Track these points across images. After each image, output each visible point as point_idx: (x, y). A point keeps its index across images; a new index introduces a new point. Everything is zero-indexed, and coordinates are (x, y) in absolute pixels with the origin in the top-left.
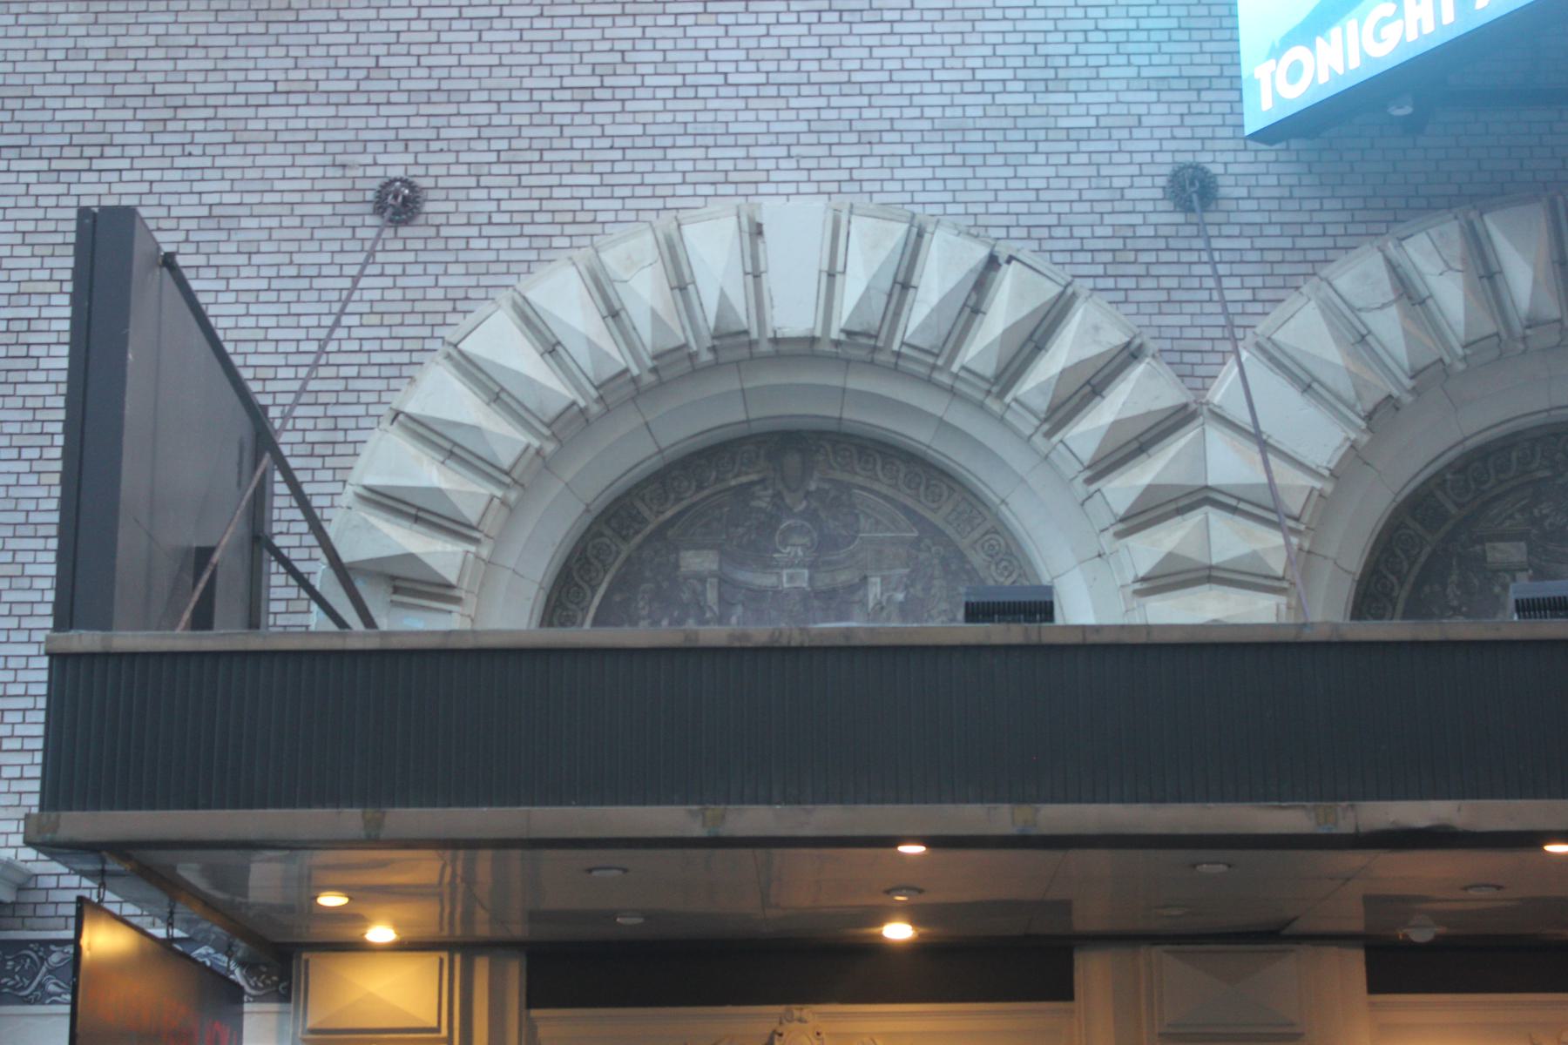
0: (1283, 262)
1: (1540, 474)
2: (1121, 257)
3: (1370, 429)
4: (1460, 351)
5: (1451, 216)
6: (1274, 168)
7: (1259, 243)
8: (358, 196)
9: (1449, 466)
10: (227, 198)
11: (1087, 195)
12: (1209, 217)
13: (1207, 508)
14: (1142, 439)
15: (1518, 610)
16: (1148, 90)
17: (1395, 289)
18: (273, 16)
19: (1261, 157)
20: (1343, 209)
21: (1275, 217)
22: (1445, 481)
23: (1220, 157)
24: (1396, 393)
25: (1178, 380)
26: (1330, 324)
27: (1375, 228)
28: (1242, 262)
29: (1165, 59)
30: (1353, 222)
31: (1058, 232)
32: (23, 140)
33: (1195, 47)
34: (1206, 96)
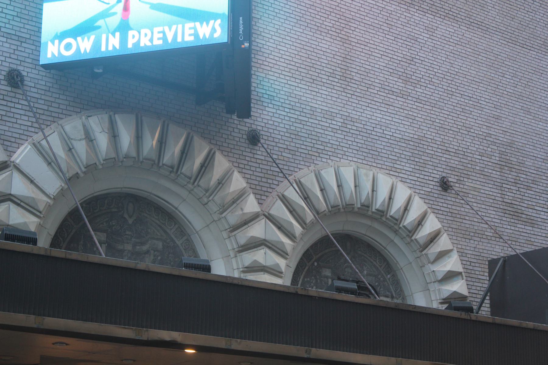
0: (43, 114)
1: (114, 210)
4: (102, 162)
6: (44, 78)
13: (9, 202)
16: (3, 36)
19: (41, 73)
21: (43, 97)
23: (26, 69)
26: (61, 142)
29: (11, 27)
30: (69, 105)
33: (22, 25)
34: (23, 45)
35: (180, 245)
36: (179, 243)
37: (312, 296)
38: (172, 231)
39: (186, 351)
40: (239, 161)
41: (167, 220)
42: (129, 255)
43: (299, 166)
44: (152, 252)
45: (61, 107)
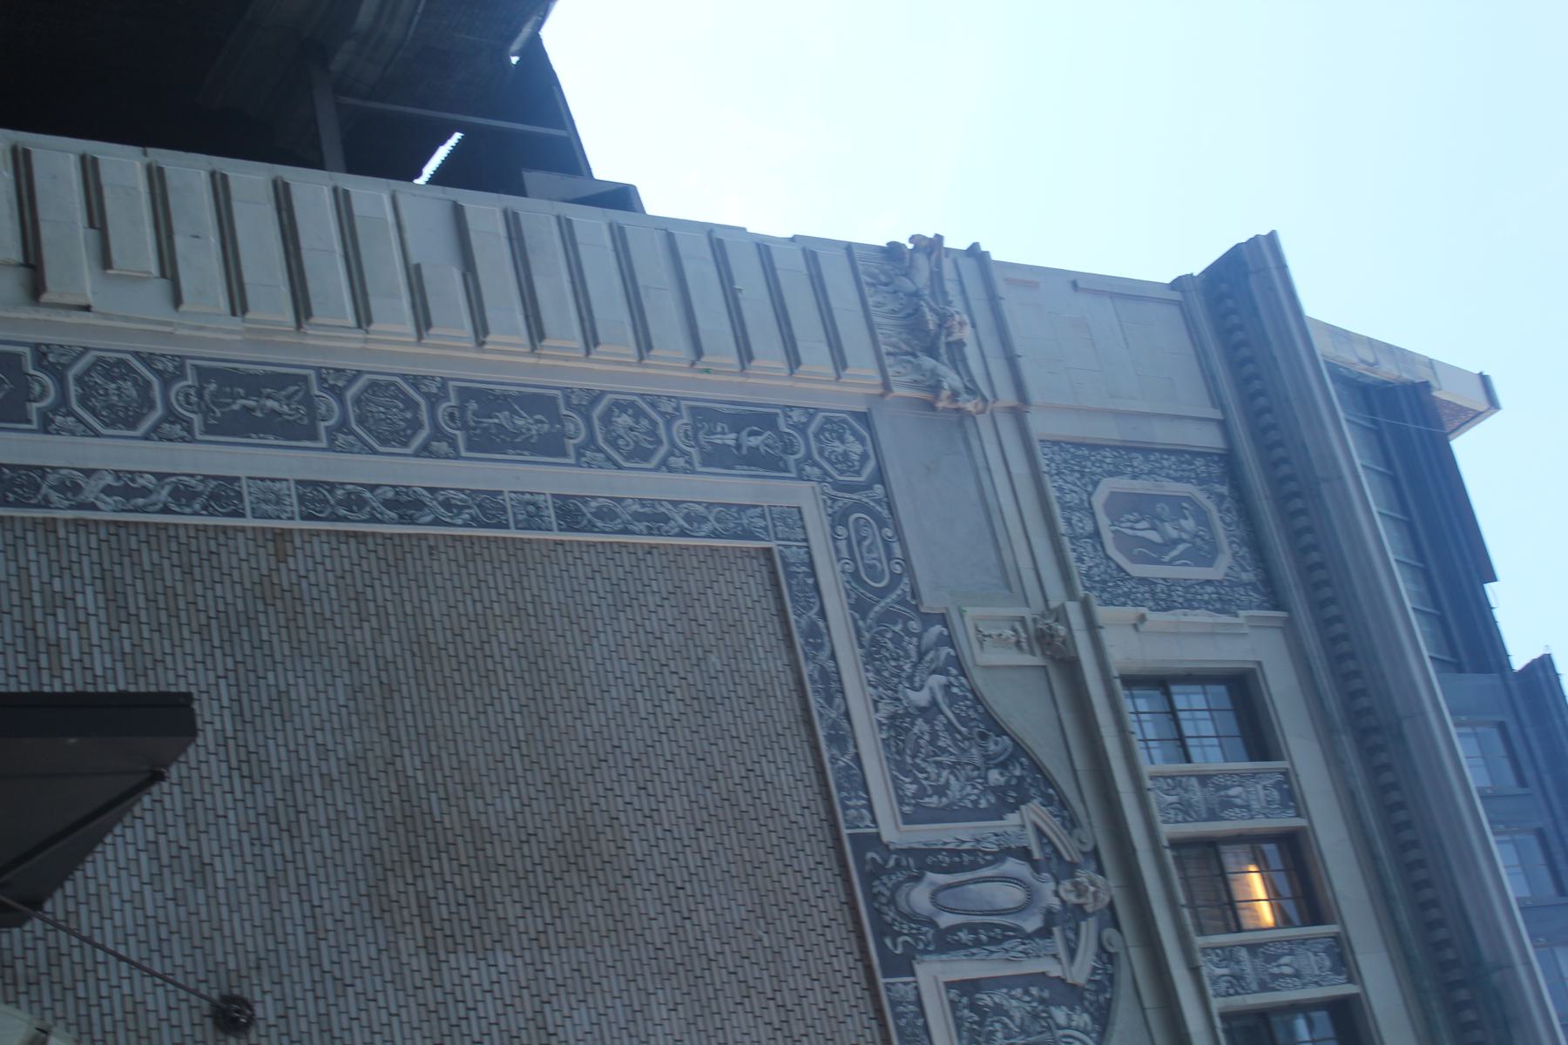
8: (234, 982)
10: (220, 877)
18: (375, 898)
32: (248, 717)
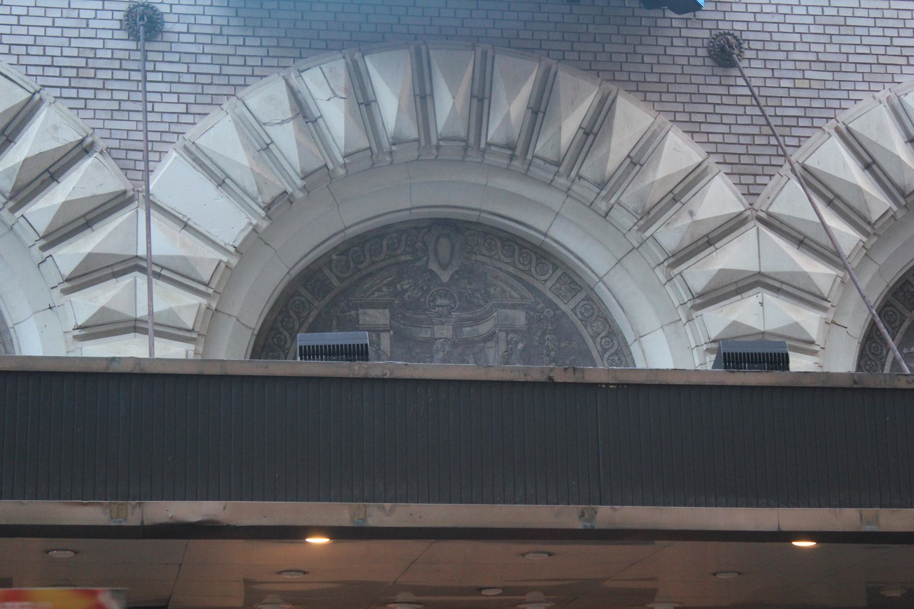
0: (211, 84)
1: (403, 258)
2: (83, 73)
3: (268, 217)
4: (341, 160)
5: (340, 55)
7: (193, 68)
9: (335, 248)
11: (58, 23)
12: (150, 46)
14: (88, 217)
15: (301, 356)
17: (293, 110)
20: (261, 46)
21: (208, 49)
22: (331, 260)
24: (290, 190)
25: (122, 173)
26: (242, 134)
27: (284, 62)
28: (179, 82)
30: (268, 56)
31: (33, 50)
35: (569, 313)
36: (566, 308)
37: (595, 386)
38: (549, 284)
39: (308, 540)
40: (688, 108)
41: (534, 263)
42: (447, 348)
43: (853, 95)
44: (502, 335)
45: (250, 62)
